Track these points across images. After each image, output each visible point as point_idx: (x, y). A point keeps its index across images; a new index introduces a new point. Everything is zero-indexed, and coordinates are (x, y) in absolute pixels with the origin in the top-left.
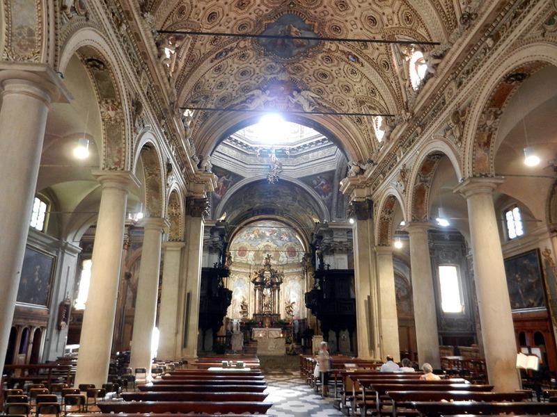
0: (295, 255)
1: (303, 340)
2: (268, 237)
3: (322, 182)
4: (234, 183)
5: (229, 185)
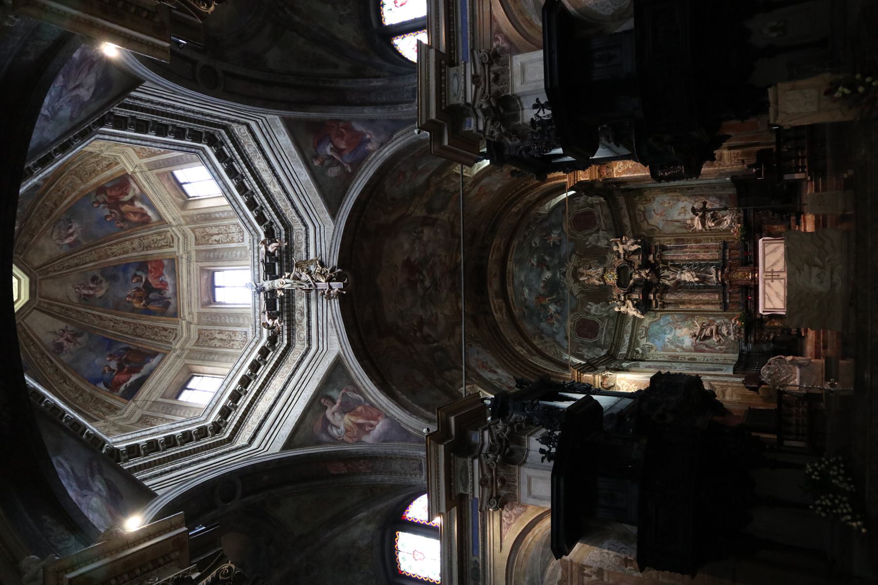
0: (591, 213)
1: (787, 177)
2: (554, 275)
3: (329, 153)
4: (352, 383)
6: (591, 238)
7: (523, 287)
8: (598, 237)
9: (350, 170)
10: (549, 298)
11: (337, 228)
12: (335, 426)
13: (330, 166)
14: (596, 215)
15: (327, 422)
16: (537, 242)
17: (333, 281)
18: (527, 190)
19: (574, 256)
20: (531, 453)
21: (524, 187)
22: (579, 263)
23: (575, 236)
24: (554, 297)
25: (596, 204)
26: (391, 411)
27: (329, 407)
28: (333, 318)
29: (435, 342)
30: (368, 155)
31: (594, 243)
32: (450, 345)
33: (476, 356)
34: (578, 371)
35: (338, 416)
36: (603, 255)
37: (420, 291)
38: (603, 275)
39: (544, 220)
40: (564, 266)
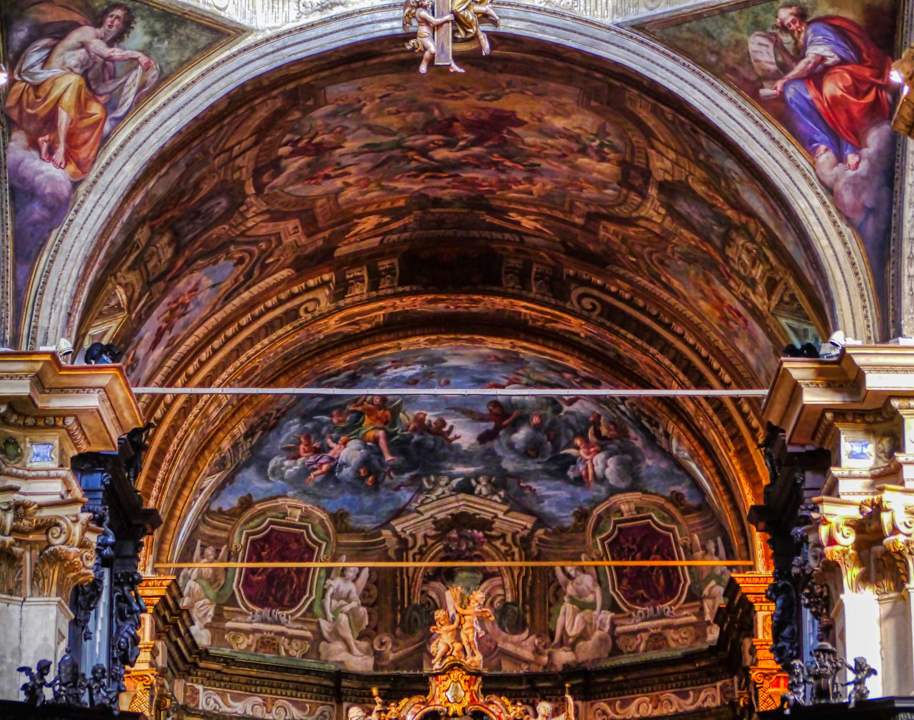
2: (464, 458)
3: (813, 52)
5: (130, 95)
6: (587, 580)
7: (422, 363)
8: (592, 606)
9: (766, 92)
10: (382, 443)
11: (605, 35)
12: (49, 55)
13: (779, 46)
14: (666, 606)
15: (61, 31)
16: (576, 407)
17: (455, 31)
18: (736, 437)
19: (528, 522)
20: (15, 608)
21: (748, 424)
22: (503, 536)
23: (596, 530)
24: (388, 458)
25: (702, 609)
26: (92, 197)
27: (100, 31)
28: (348, 15)
29: (259, 189)
30: (803, 146)
31: (570, 590)
32: (247, 219)
33: (207, 282)
34: (163, 598)
35: (74, 58)
36: (528, 621)
37: (419, 141)
38: (460, 666)
39: (651, 440)
40: (495, 488)
